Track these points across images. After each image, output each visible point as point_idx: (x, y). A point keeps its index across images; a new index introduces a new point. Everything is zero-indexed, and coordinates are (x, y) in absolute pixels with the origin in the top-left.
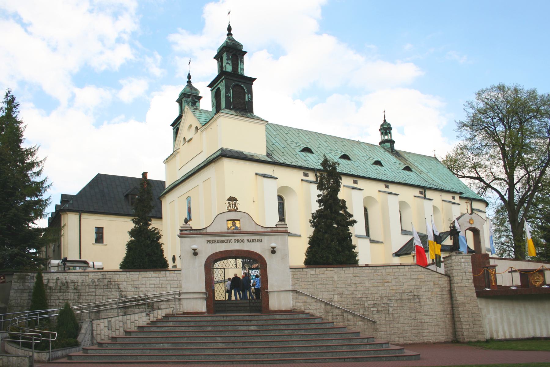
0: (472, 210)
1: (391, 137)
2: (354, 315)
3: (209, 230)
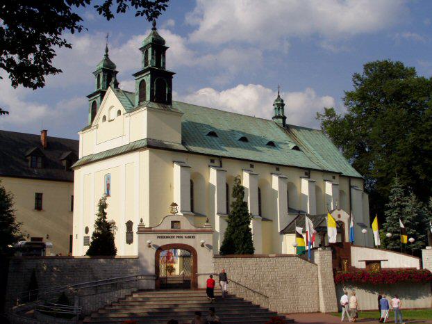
0: (350, 187)
1: (283, 112)
2: (254, 292)
3: (158, 228)
